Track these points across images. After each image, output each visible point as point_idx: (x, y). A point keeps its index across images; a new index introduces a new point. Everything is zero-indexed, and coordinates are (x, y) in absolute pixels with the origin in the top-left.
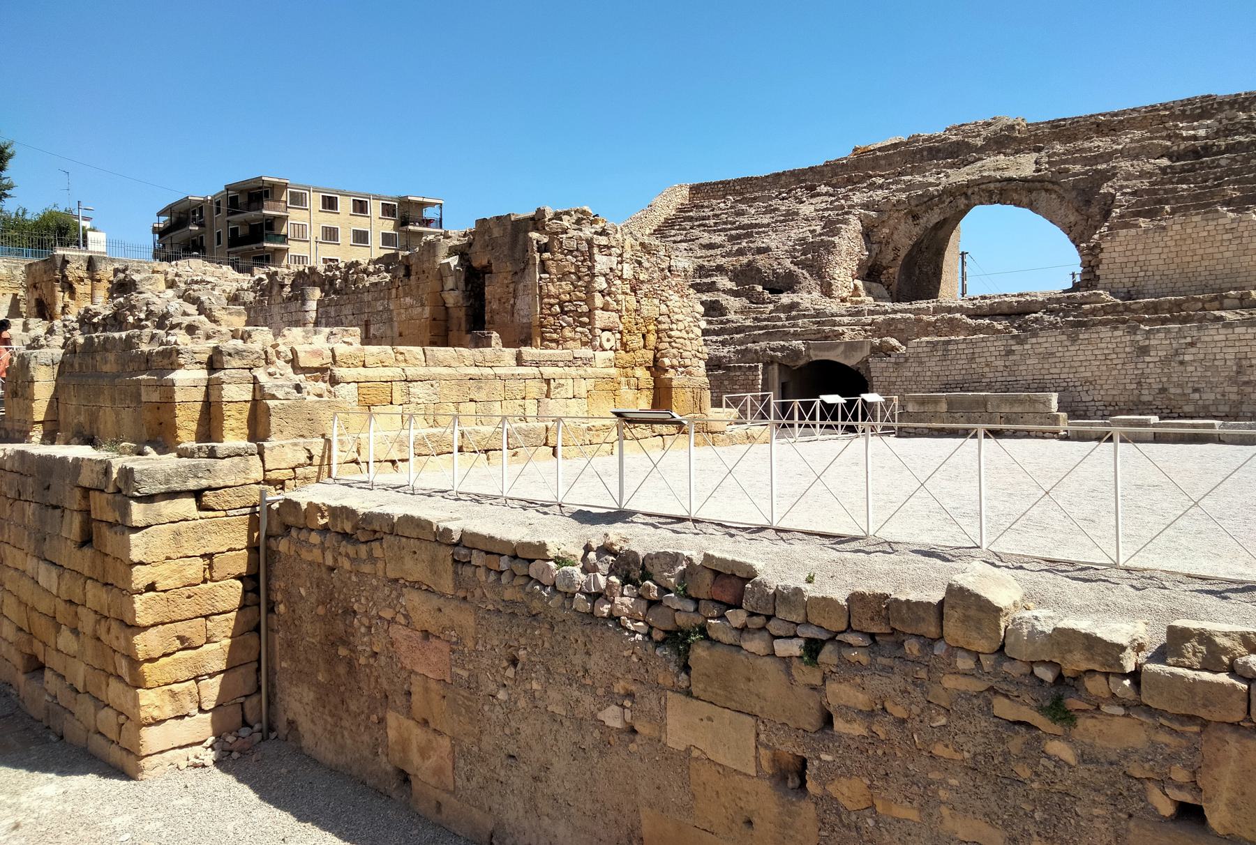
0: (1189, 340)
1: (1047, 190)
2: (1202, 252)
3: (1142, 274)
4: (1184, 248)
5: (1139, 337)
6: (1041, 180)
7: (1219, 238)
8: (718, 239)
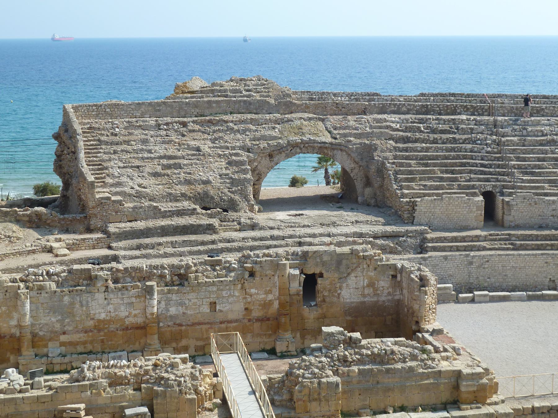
0: (487, 260)
1: (341, 150)
2: (455, 210)
3: (432, 217)
4: (449, 208)
5: (469, 258)
6: (340, 145)
7: (462, 205)
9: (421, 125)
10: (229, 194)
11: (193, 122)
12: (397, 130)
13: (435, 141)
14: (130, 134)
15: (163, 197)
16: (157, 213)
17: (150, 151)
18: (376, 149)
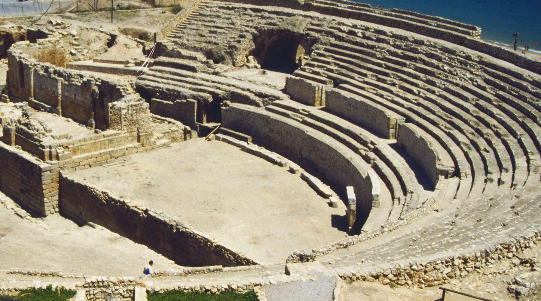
6: (302, 35)
8: (205, 31)
9: (361, 31)
10: (223, 53)
11: (251, 9)
12: (344, 32)
13: (356, 43)
14: (217, 12)
15: (192, 48)
16: (180, 56)
17: (214, 22)
18: (318, 42)
